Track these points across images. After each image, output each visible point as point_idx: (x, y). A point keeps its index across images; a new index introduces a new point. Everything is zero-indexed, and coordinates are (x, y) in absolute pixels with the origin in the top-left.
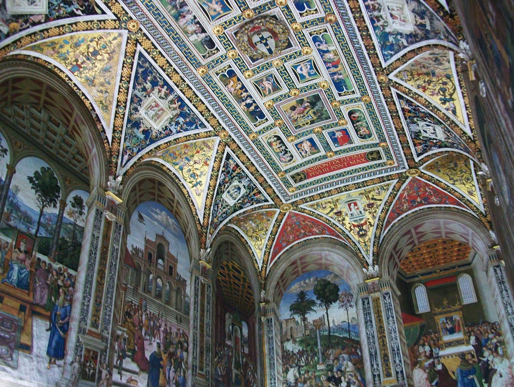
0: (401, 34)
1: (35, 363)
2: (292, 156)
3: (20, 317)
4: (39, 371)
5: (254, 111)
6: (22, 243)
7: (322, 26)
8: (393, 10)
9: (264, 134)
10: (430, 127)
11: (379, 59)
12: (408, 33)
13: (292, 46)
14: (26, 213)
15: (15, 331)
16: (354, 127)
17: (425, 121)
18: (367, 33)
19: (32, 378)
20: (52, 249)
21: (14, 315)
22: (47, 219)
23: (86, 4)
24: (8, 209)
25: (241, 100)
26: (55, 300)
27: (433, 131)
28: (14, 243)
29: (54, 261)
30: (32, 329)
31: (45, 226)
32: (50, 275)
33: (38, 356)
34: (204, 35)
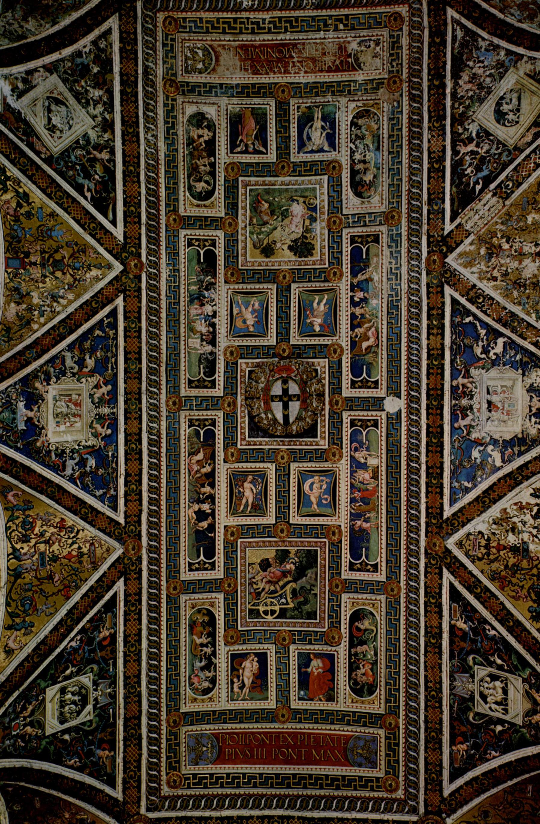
0: (494, 442)
2: (213, 681)
5: (203, 531)
7: (374, 413)
8: (495, 392)
9: (192, 596)
10: (498, 684)
11: (442, 498)
12: (508, 437)
13: (316, 437)
16: (350, 658)
17: (491, 664)
18: (439, 440)
23: (104, 195)
25: (195, 496)
27: (500, 696)
34: (209, 348)
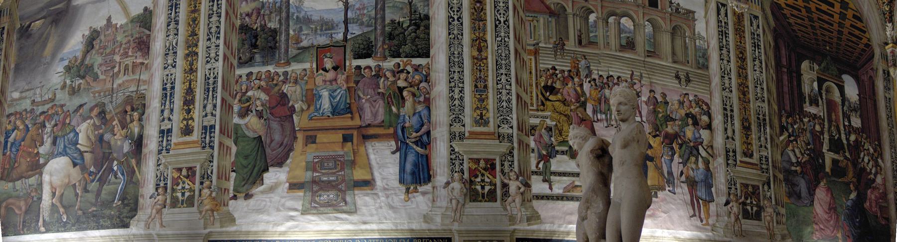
1: (383, 199)
3: (345, 149)
4: (391, 207)
6: (326, 60)
14: (322, 19)
15: (342, 169)
19: (382, 218)
20: (376, 45)
21: (336, 151)
22: (359, 9)
24: (294, 31)
26: (398, 110)
28: (315, 66)
29: (385, 58)
30: (368, 159)
31: (355, 21)
32: (382, 79)
33: (385, 189)
